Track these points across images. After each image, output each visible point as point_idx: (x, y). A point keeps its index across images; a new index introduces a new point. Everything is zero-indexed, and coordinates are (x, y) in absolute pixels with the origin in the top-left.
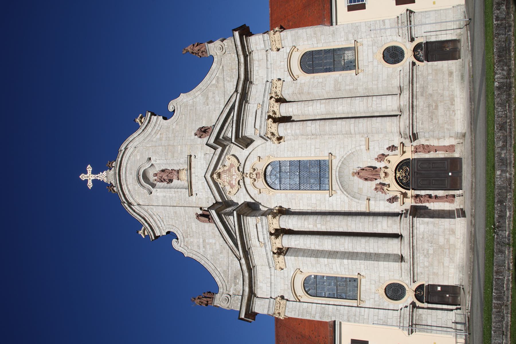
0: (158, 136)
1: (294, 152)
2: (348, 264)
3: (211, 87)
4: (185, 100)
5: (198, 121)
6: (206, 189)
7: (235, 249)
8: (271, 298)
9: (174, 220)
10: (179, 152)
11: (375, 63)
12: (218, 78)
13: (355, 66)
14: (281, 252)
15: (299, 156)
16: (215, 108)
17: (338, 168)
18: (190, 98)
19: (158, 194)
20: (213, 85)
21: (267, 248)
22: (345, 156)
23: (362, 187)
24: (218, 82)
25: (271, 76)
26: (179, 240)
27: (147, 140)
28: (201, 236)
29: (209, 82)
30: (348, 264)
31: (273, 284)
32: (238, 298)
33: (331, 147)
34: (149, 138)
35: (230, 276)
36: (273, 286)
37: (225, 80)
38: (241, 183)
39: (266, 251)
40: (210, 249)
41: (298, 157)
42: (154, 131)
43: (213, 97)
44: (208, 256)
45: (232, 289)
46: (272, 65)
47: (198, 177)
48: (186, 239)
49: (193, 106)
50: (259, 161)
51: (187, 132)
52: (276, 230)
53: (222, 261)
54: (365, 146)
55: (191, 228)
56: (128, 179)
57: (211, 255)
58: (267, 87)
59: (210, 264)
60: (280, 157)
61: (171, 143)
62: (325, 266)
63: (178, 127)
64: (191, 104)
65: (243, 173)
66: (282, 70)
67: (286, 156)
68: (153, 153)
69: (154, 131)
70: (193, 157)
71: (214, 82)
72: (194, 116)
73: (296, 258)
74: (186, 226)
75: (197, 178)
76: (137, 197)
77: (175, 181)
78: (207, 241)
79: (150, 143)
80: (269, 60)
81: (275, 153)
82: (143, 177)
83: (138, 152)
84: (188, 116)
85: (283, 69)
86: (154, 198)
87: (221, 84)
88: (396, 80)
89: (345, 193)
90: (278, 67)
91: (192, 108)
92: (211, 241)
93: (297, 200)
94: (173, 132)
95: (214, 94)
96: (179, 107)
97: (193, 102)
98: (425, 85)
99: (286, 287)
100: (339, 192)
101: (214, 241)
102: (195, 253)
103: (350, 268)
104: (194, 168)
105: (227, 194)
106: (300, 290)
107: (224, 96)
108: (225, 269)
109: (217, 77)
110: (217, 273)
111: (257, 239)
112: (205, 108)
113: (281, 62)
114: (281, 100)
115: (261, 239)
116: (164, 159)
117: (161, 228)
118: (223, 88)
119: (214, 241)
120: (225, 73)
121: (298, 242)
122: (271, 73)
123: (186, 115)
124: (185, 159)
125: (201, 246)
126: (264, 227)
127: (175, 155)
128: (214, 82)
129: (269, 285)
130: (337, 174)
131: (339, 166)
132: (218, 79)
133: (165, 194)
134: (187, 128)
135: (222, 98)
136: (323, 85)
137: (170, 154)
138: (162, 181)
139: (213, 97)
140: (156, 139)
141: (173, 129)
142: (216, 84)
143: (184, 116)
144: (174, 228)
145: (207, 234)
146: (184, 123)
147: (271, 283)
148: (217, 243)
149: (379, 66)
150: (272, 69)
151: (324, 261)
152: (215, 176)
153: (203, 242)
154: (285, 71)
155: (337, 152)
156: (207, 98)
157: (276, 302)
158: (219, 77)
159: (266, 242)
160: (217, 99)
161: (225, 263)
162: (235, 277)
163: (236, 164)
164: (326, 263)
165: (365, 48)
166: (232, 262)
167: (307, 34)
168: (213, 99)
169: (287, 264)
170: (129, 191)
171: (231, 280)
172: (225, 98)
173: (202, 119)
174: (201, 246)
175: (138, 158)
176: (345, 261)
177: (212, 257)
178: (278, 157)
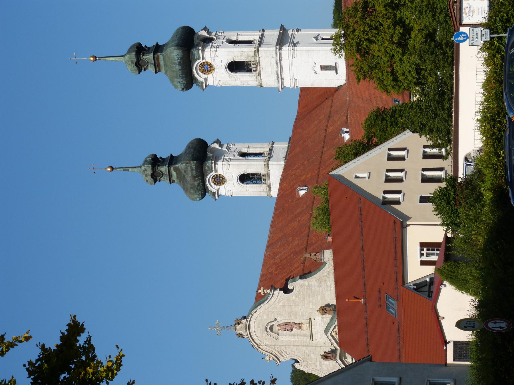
0: (281, 304)
5: (313, 296)
6: (324, 338)
24: (329, 275)
27: (272, 307)
42: (277, 301)
49: (309, 287)
51: (306, 303)
56: (256, 331)
64: (307, 286)
69: (277, 301)
72: (311, 293)
74: (306, 355)
76: (264, 340)
79: (275, 309)
95: (326, 281)
104: (314, 325)
112: (319, 289)
116: (288, 319)
124: (307, 320)
127: (297, 317)
133: (289, 339)
134: (305, 300)
138: (285, 330)
141: (293, 300)
143: (301, 292)
144: (296, 356)
156: (321, 283)
168: (325, 284)
170: (258, 337)
175: (265, 317)
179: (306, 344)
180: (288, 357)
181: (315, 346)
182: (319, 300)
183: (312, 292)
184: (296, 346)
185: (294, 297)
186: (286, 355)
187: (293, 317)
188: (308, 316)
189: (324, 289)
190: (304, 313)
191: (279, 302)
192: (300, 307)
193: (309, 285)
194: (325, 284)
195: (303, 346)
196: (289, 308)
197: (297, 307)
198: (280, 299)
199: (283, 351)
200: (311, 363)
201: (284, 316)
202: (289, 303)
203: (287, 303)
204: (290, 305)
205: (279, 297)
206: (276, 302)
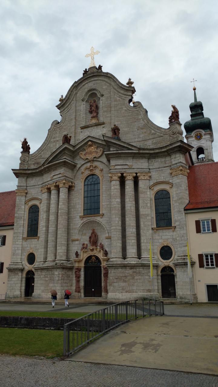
0: (118, 99)
3: (150, 130)
4: (141, 113)
8: (27, 186)
10: (107, 115)
11: (160, 241)
12: (155, 134)
13: (159, 227)
16: (135, 135)
17: (95, 220)
18: (143, 116)
20: (151, 132)
22: (102, 224)
25: (154, 171)
26: (57, 125)
27: (115, 91)
29: (153, 128)
33: (108, 215)
34: (117, 92)
35: (39, 160)
37: (154, 139)
39: (49, 181)
41: (102, 194)
43: (142, 133)
44: (49, 145)
45: (31, 162)
46: (161, 171)
48: (58, 129)
50: (100, 170)
51: (120, 119)
54: (108, 236)
55: (64, 131)
56: (91, 83)
57: (50, 146)
59: (45, 146)
61: (113, 109)
63: (124, 111)
65: (93, 161)
66: (158, 178)
68: (107, 97)
69: (121, 95)
70: (103, 126)
71: (153, 131)
73: (46, 199)
75: (91, 131)
77: (90, 116)
78: (57, 143)
81: (105, 180)
82: (92, 93)
83: (108, 86)
84: (131, 117)
88: (147, 255)
91: (136, 119)
93: (78, 196)
96: (138, 109)
97: (140, 119)
98: (141, 274)
99: (33, 195)
105: (80, 152)
106: (31, 203)
107: (143, 140)
110: (40, 152)
111: (54, 175)
114: (136, 180)
115: (55, 177)
118: (148, 138)
120: (158, 138)
122: (156, 171)
125: (55, 140)
126: (59, 179)
127: (105, 113)
128: (153, 131)
129: (34, 184)
131: (97, 221)
132: (155, 134)
134: (123, 118)
135: (142, 139)
137: (106, 109)
139: (142, 133)
141: (122, 108)
142: (152, 133)
143: (131, 114)
144: (64, 120)
149: (159, 243)
152: (90, 143)
155: (105, 219)
156: (142, 129)
157: (24, 190)
158: (156, 135)
160: (141, 136)
162: (38, 163)
163: (97, 156)
165: (171, 233)
172: (142, 142)
173: (128, 127)
174: (55, 140)
175: (104, 87)
179: (77, 125)
182: (123, 129)
183: (132, 122)
185: (126, 109)
187: (106, 109)
189: (135, 132)
190: (110, 118)
191: (120, 97)
192: (116, 114)
196: (115, 105)
197: (116, 112)
202: (120, 104)
203: (119, 103)
205: (125, 96)
206: (120, 94)
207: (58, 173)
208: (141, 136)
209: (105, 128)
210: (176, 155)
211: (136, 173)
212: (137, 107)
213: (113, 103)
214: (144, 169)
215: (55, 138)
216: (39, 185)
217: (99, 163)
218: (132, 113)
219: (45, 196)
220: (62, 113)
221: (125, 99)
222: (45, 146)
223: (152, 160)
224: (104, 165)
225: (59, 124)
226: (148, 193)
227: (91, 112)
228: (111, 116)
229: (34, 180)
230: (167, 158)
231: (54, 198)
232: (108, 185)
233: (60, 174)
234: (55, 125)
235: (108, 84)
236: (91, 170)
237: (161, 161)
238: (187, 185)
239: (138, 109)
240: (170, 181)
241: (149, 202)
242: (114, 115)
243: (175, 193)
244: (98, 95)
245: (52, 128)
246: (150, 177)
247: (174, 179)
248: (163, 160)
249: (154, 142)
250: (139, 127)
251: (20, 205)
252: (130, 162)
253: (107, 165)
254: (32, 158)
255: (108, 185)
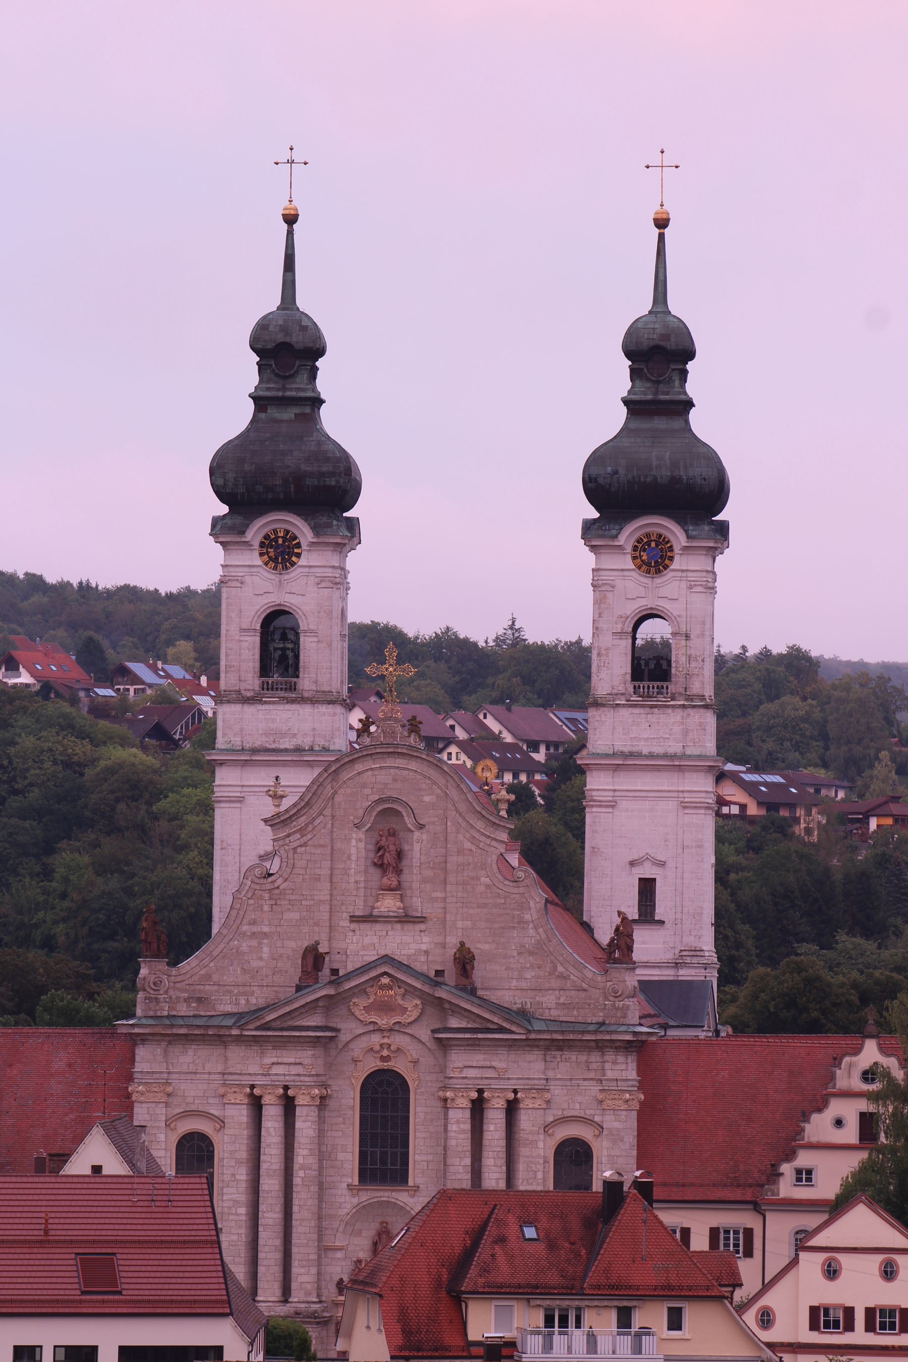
1: (423, 1125)
2: (237, 1214)
3: (552, 962)
7: (258, 1024)
9: (302, 872)
14: (256, 1104)
15: (418, 1134)
18: (535, 916)
19: (354, 842)
20: (555, 968)
21: (259, 1077)
23: (363, 1235)
24: (559, 977)
26: (262, 881)
27: (460, 820)
28: (273, 929)
30: (237, 1214)
31: (193, 1075)
32: (163, 1010)
35: (202, 987)
36: (189, 1077)
37: (561, 992)
38: (371, 1027)
40: (250, 946)
43: (532, 966)
45: (178, 993)
46: (576, 1088)
47: (385, 937)
49: (519, 923)
51: (471, 911)
52: (293, 1099)
53: (229, 971)
57: (238, 948)
58: (536, 1082)
59: (222, 946)
60: (416, 1099)
62: (233, 1175)
63: (482, 888)
64: (523, 917)
66: (565, 1106)
67: (418, 1109)
69: (477, 835)
70: (422, 926)
74: (292, 897)
76: (349, 791)
78: (265, 941)
80: (586, 1083)
81: (422, 1090)
85: (567, 1107)
86: (347, 832)
87: (555, 983)
89: (354, 1210)
90: (572, 1099)
91: (516, 920)
92: (266, 949)
93: (342, 1126)
94: (472, 879)
95: (539, 968)
96: (522, 890)
99: (190, 1100)
100: (355, 1200)
101: (265, 956)
102: (241, 913)
103: (231, 1217)
104: (402, 929)
107: (533, 988)
108: (215, 977)
109: (569, 976)
111: (275, 1060)
113: (580, 1103)
114: (512, 1108)
116: (422, 861)
117: (287, 840)
118: (547, 986)
119: (265, 956)
121: (273, 1134)
123: (504, 906)
125: (255, 929)
126: (297, 1078)
127: (428, 885)
130: (385, 1199)
132: (565, 978)
133: (354, 858)
134: (479, 910)
136: (530, 1181)
140: (461, 842)
141: (478, 878)
142: (557, 974)
144: (289, 870)
145: (279, 944)
146: (490, 901)
147: (196, 1073)
148: (262, 964)
150: (569, 1088)
151: (243, 1174)
153: (262, 933)
154: (563, 1110)
155: (421, 1199)
156: (531, 953)
159: (271, 1077)
160: (529, 975)
161: (225, 978)
162: (201, 998)
164: (238, 1177)
166: (229, 992)
167: (618, 1156)
168: (528, 966)
169: (233, 1107)
171: (194, 990)
174: (255, 929)
176: (242, 1210)
177: (234, 951)
178: (416, 1094)
179: (335, 902)
180: (287, 848)
181: (330, 926)
184: (331, 876)
185: (487, 880)
186: (295, 844)
188: (431, 913)
190: (442, 905)
193: (525, 923)
194: (528, 966)
195: (331, 895)
197: (460, 888)
198: (482, 843)
199: (309, 836)
200: (266, 908)
201: (432, 850)
204: (466, 868)
207: (292, 1060)
208: (529, 975)
209: (426, 932)
210: (618, 1057)
211: (515, 1092)
212: (521, 884)
213: (453, 860)
214: (534, 1079)
215: (254, 923)
216: (209, 1073)
217: (407, 1039)
218: (505, 898)
219: (240, 1115)
220: (280, 843)
221: (486, 848)
222: (222, 946)
223: (553, 1053)
224: (421, 1046)
225: (270, 879)
226: (541, 1145)
227: (381, 866)
228: (444, 899)
229: (191, 1052)
230: (592, 1053)
231: (275, 1128)
232: (432, 1107)
233: (300, 1064)
234: (256, 880)
235: (439, 791)
236: (384, 1059)
237: (577, 1058)
238: (636, 1133)
239: (522, 890)
240: (597, 1119)
241: (541, 1168)
242: (454, 900)
243: (605, 1152)
244: (409, 822)
245: (247, 888)
246: (548, 1102)
247: (607, 1118)
248: (583, 1058)
249: (562, 1000)
250: (524, 946)
251: (155, 1131)
252: (500, 1060)
253: (430, 1050)
254: (179, 979)
255: (432, 1107)
